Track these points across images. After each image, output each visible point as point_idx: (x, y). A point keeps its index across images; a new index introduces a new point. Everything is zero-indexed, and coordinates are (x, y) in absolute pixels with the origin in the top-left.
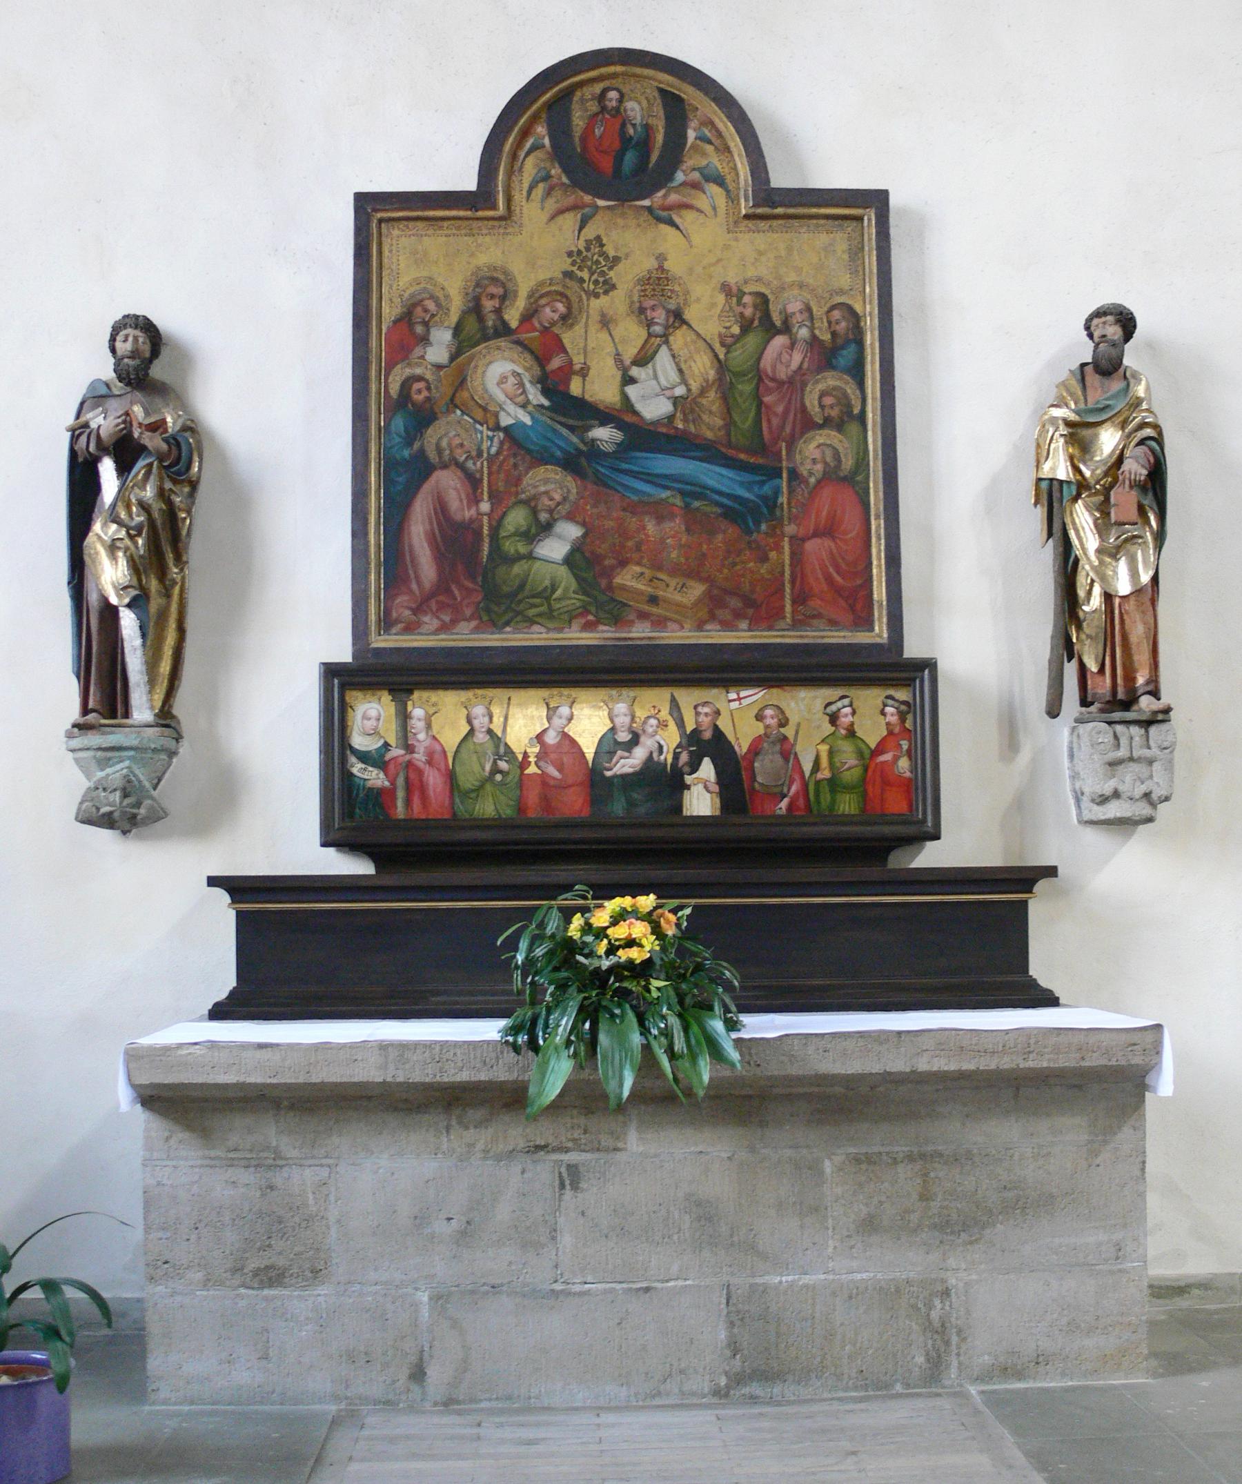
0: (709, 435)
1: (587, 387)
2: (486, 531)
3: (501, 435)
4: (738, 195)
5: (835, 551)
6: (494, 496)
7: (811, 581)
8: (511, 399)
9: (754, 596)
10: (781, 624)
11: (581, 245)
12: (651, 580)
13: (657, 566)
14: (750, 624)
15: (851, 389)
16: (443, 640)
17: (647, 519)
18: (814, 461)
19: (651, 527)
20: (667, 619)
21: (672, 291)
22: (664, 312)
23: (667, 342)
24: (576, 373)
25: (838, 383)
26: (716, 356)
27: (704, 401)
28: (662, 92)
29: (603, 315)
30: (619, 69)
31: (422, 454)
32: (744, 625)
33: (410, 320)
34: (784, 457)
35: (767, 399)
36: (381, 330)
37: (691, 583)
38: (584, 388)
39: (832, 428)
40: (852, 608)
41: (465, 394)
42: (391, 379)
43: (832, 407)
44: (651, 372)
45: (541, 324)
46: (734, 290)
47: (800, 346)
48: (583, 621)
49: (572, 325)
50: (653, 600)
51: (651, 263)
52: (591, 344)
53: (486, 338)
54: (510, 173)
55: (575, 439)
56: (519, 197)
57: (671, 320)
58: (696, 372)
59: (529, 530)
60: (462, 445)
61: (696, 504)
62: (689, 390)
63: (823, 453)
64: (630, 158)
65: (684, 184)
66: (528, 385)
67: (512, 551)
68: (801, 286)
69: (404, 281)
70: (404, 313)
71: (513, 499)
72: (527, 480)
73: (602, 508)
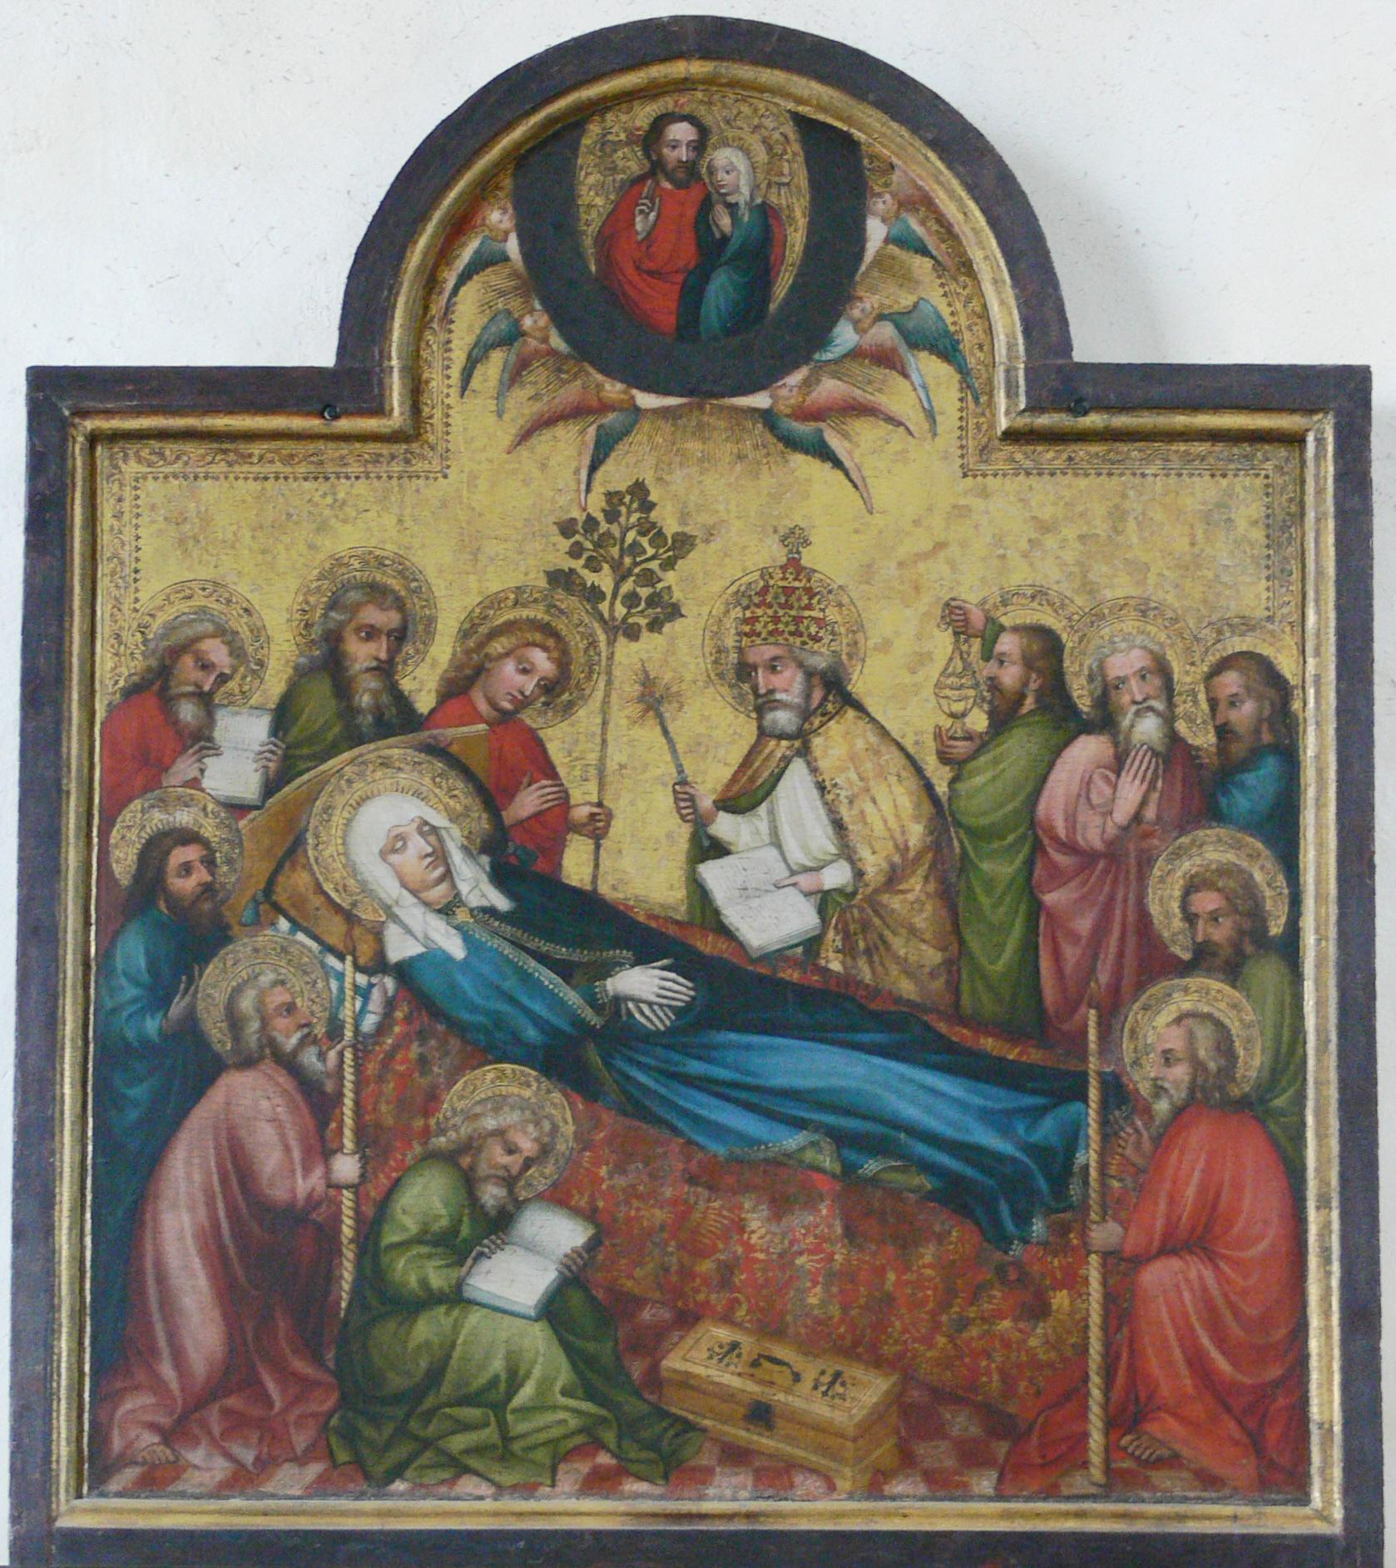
0: (907, 988)
1: (606, 862)
2: (347, 1231)
3: (390, 983)
4: (990, 382)
5: (1215, 1291)
6: (370, 1142)
7: (1154, 1366)
8: (414, 893)
9: (1012, 1409)
11: (596, 504)
12: (755, 1364)
13: (771, 1326)
14: (1001, 1479)
15: (1264, 873)
18: (1168, 1058)
19: (757, 1223)
21: (821, 623)
22: (800, 677)
23: (805, 752)
24: (577, 828)
25: (1230, 857)
26: (929, 787)
27: (895, 903)
28: (800, 121)
29: (647, 682)
30: (698, 68)
31: (190, 1029)
32: (985, 1483)
33: (164, 688)
35: (1049, 898)
36: (92, 714)
38: (597, 866)
41: (301, 879)
43: (1214, 917)
44: (763, 827)
45: (494, 705)
46: (977, 619)
47: (1139, 764)
49: (568, 709)
50: (761, 1415)
51: (771, 553)
52: (615, 757)
53: (355, 738)
54: (420, 323)
55: (572, 997)
56: (441, 382)
57: (817, 695)
58: (879, 828)
59: (454, 1230)
60: (290, 1008)
61: (871, 1166)
62: (859, 874)
63: (1191, 1034)
64: (721, 290)
65: (856, 354)
66: (457, 858)
67: (413, 1280)
68: (1145, 610)
69: (151, 589)
70: (149, 669)
71: (418, 1149)
72: (454, 1100)
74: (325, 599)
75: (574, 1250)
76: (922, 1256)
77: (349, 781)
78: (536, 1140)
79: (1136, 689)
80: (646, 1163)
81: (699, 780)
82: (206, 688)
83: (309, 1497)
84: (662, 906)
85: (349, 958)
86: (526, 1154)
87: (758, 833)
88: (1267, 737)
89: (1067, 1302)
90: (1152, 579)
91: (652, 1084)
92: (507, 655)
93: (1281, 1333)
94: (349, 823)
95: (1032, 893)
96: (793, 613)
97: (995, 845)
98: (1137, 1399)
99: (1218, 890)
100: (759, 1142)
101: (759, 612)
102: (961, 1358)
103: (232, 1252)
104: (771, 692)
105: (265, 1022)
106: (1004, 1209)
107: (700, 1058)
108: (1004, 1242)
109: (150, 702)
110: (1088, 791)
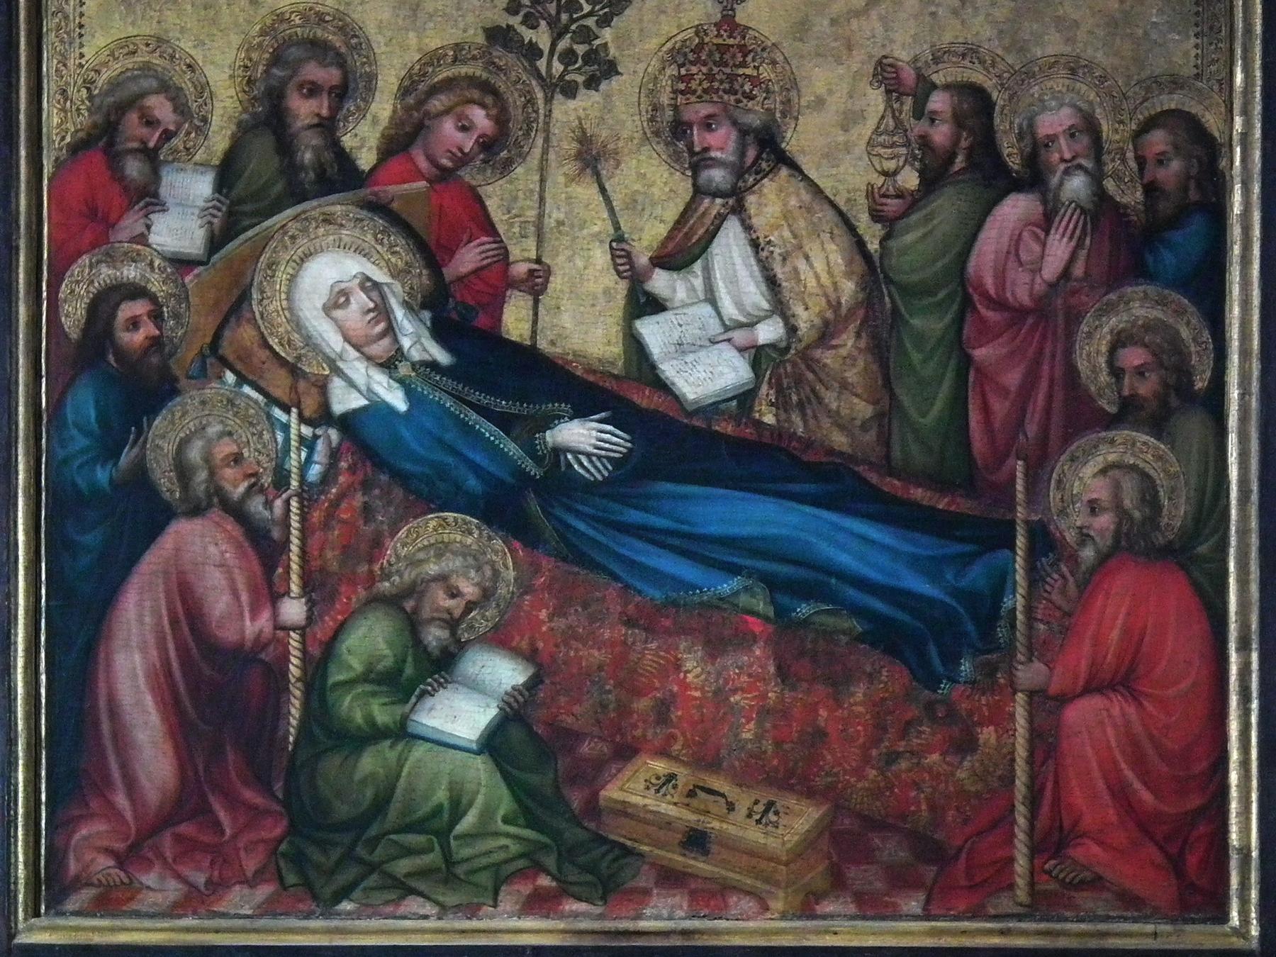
0: (839, 440)
2: (294, 670)
3: (334, 434)
5: (1138, 728)
8: (357, 348)
10: (1004, 904)
12: (691, 794)
13: (707, 760)
14: (928, 901)
15: (1189, 329)
16: (188, 930)
17: (683, 645)
18: (1094, 508)
19: (693, 666)
20: (726, 888)
21: (755, 81)
22: (734, 135)
23: (739, 209)
24: (513, 284)
25: (1157, 313)
26: (860, 244)
27: (828, 358)
29: (584, 140)
31: (140, 477)
32: (914, 904)
33: (111, 144)
34: (1020, 496)
35: (980, 353)
37: (792, 801)
38: (535, 322)
39: (1137, 426)
40: (1177, 866)
41: (246, 334)
42: (64, 289)
43: (1140, 372)
44: (698, 283)
45: (432, 160)
46: (909, 75)
47: (1067, 220)
48: (526, 889)
49: (506, 167)
50: (696, 841)
52: (554, 214)
57: (751, 154)
58: (812, 283)
60: (237, 459)
61: (804, 610)
62: (792, 330)
66: (399, 313)
68: (1075, 68)
69: (95, 45)
70: (95, 126)
71: (362, 593)
72: (399, 546)
73: (575, 618)
74: (267, 56)
75: (514, 688)
76: (853, 694)
77: (293, 238)
78: (477, 584)
79: (1065, 147)
80: (585, 607)
81: (636, 237)
82: (151, 144)
83: (261, 916)
84: (600, 360)
85: (294, 410)
86: (469, 597)
87: (693, 289)
88: (1193, 195)
89: (993, 740)
90: (1081, 35)
91: (591, 532)
92: (447, 111)
93: (1200, 766)
94: (292, 279)
95: (962, 349)
96: (728, 70)
97: (926, 301)
98: (1061, 827)
99: (1146, 346)
100: (694, 587)
101: (694, 70)
102: (891, 789)
103: (182, 688)
104: (706, 150)
105: (212, 473)
106: (933, 651)
107: (636, 508)
108: (932, 682)
109: (96, 158)
110: (1017, 250)
